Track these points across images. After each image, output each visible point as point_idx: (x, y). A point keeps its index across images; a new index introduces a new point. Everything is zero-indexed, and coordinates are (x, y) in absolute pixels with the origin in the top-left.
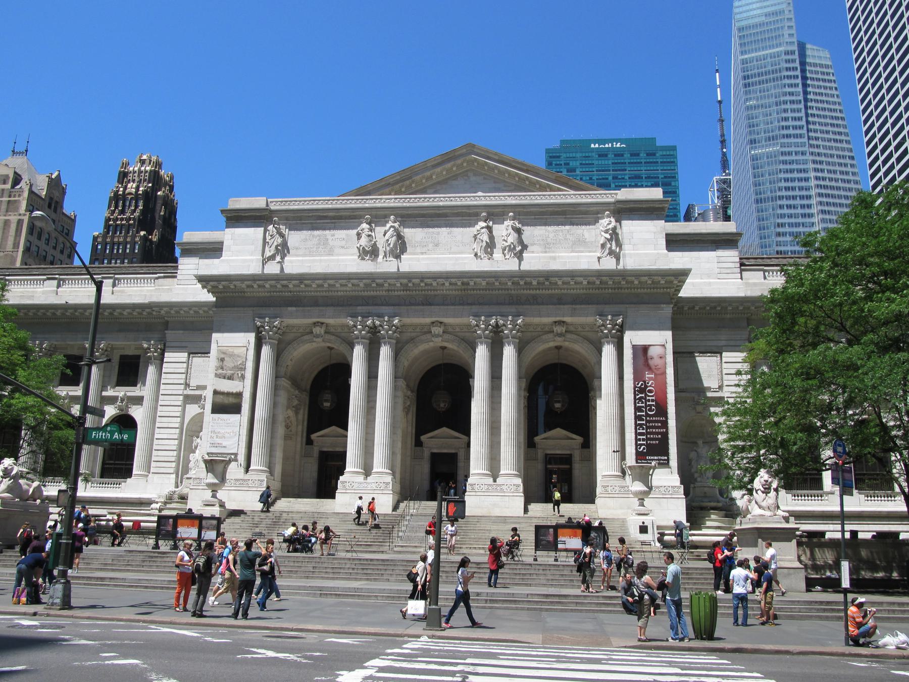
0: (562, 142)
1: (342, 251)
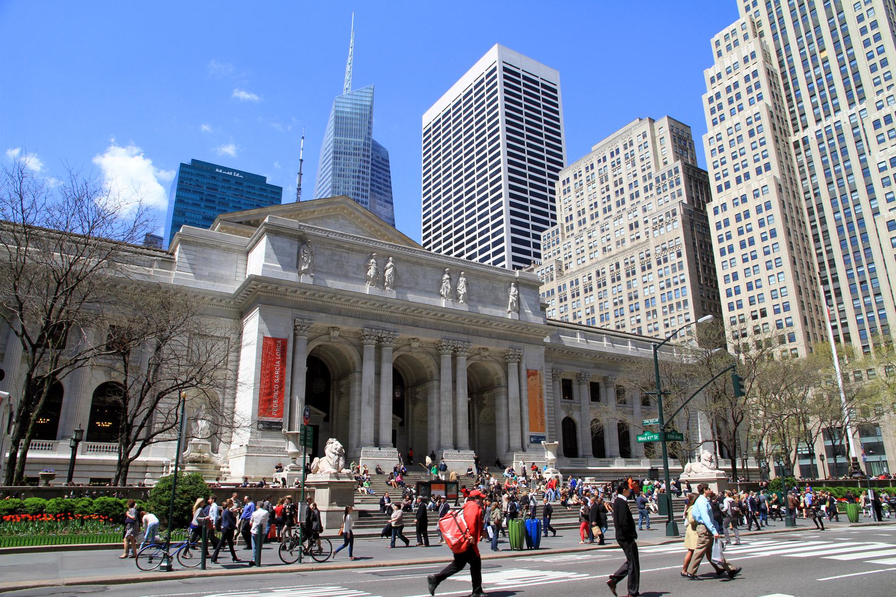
0: (193, 160)
1: (354, 276)
